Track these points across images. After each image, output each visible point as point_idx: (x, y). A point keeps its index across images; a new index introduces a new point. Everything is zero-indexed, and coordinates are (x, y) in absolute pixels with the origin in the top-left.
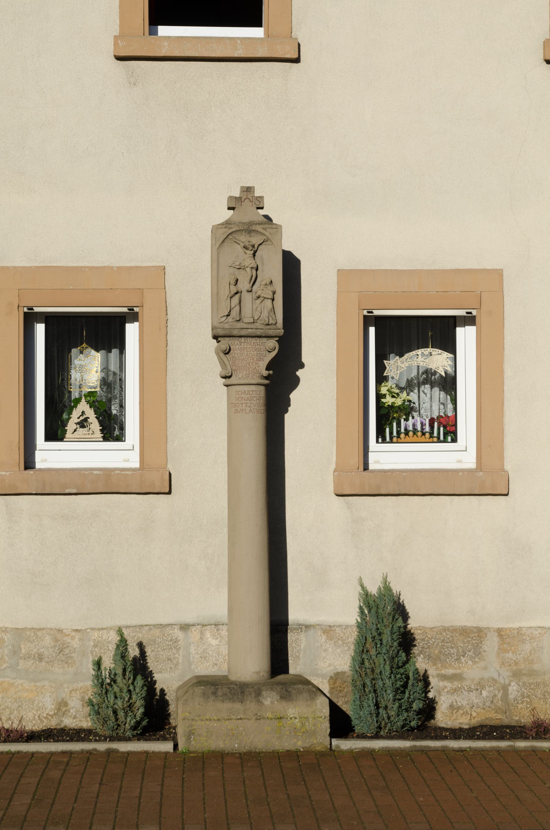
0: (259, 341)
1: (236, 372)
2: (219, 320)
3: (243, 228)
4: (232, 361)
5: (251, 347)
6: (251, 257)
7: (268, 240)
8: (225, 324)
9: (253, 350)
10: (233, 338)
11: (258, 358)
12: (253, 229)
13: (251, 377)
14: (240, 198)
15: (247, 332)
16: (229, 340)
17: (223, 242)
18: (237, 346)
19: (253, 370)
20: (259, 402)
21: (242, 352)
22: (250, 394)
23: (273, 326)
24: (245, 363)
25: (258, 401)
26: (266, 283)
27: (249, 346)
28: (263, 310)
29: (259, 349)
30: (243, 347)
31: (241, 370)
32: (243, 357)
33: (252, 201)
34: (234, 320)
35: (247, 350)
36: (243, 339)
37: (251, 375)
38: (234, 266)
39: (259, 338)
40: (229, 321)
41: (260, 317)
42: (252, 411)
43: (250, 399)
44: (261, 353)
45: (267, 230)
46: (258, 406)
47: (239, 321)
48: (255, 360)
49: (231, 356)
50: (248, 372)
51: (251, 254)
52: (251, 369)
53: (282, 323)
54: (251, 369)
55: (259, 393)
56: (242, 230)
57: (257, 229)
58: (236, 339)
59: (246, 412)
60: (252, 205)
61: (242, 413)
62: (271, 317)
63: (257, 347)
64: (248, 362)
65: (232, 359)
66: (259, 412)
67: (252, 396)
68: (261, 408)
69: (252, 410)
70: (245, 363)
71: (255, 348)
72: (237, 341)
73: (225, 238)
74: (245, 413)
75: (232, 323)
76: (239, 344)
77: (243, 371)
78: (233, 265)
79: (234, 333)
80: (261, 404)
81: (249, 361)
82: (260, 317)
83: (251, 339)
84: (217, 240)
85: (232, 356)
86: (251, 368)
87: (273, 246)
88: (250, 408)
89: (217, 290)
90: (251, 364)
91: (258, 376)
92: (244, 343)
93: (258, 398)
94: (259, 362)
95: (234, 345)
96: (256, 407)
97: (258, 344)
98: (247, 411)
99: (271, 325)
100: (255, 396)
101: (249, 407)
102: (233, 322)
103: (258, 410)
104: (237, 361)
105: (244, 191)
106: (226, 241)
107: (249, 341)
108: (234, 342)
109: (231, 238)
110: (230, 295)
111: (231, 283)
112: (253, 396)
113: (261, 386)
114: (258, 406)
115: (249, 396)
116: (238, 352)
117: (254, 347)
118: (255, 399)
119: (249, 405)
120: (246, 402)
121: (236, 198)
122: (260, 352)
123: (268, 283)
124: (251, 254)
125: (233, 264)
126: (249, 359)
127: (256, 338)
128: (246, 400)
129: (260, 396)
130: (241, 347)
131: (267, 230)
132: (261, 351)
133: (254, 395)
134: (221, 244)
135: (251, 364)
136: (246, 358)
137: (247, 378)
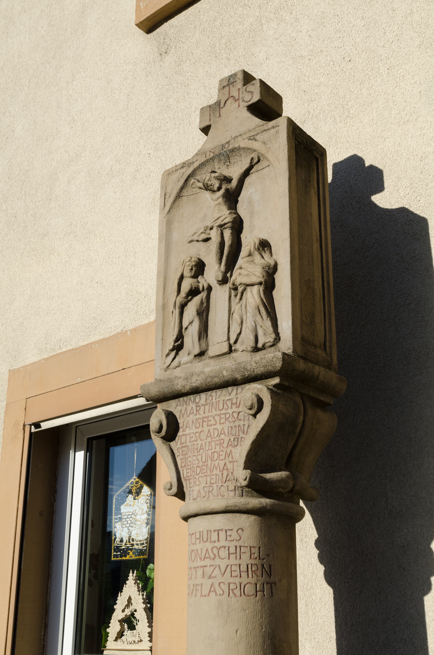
0: (236, 394)
1: (188, 482)
2: (165, 363)
3: (212, 155)
4: (181, 457)
5: (218, 412)
6: (219, 204)
7: (261, 158)
8: (175, 370)
9: (223, 420)
10: (185, 398)
11: (232, 439)
12: (231, 147)
13: (215, 492)
14: (218, 103)
15: (203, 376)
16: (177, 406)
17: (179, 196)
18: (191, 416)
19: (220, 474)
20: (237, 562)
21: (200, 430)
22: (213, 539)
23: (269, 350)
24: (204, 456)
25: (233, 560)
26: (250, 252)
27: (214, 413)
28: (244, 317)
29: (235, 415)
30: (203, 415)
31: (197, 477)
32: (199, 442)
33: (237, 98)
34: (192, 356)
35: (210, 423)
36: (203, 395)
37: (215, 486)
38: (196, 239)
39: (235, 387)
40: (182, 362)
41: (240, 333)
42: (215, 591)
43: (212, 556)
44: (239, 426)
45: (258, 137)
46: (234, 574)
47: (203, 357)
48: (225, 445)
49: (179, 443)
50: (209, 478)
51: (218, 199)
52: (215, 472)
53: (291, 340)
54: (215, 472)
55: (235, 536)
56: (213, 159)
57: (237, 146)
58: (190, 399)
59: (203, 594)
60: (239, 106)
61: (196, 596)
62: (261, 327)
63: (230, 411)
64: (210, 452)
65: (181, 452)
66: (237, 592)
67: (216, 544)
68: (245, 579)
69: (217, 586)
70: (204, 456)
71: (225, 414)
72: (191, 405)
73: (182, 188)
74: (202, 596)
75: (188, 365)
76: (195, 412)
77: (200, 479)
78: (195, 238)
79: (178, 384)
80: (244, 568)
81: (213, 450)
82: (240, 333)
83: (219, 392)
84: (167, 197)
85: (181, 443)
86: (216, 469)
87: (271, 166)
88: (211, 581)
89: (164, 298)
90: (216, 455)
91: (232, 487)
92: (205, 405)
93: (232, 550)
94: (233, 450)
95: (185, 415)
96: (227, 579)
97: (232, 404)
98: (205, 591)
99: (264, 348)
100: (227, 544)
101: (210, 577)
102: (191, 362)
103: (232, 586)
104: (190, 454)
105: (224, 87)
106: (185, 193)
107: (214, 398)
108: (186, 408)
109: (192, 184)
110: (178, 299)
111: (185, 274)
112: (218, 545)
113: (244, 516)
114: (234, 574)
115: (209, 545)
116: (191, 431)
117: (223, 412)
118: (224, 553)
119: (209, 570)
120: (202, 563)
121: (210, 106)
122: (237, 423)
123: (252, 249)
124: (218, 199)
125: (195, 233)
126: (213, 444)
127: (230, 389)
128: (203, 558)
129: (238, 544)
130: (198, 416)
131: (258, 137)
132: (240, 420)
133: (223, 543)
134: (174, 201)
135: (216, 455)
136: (207, 444)
137: (207, 496)
